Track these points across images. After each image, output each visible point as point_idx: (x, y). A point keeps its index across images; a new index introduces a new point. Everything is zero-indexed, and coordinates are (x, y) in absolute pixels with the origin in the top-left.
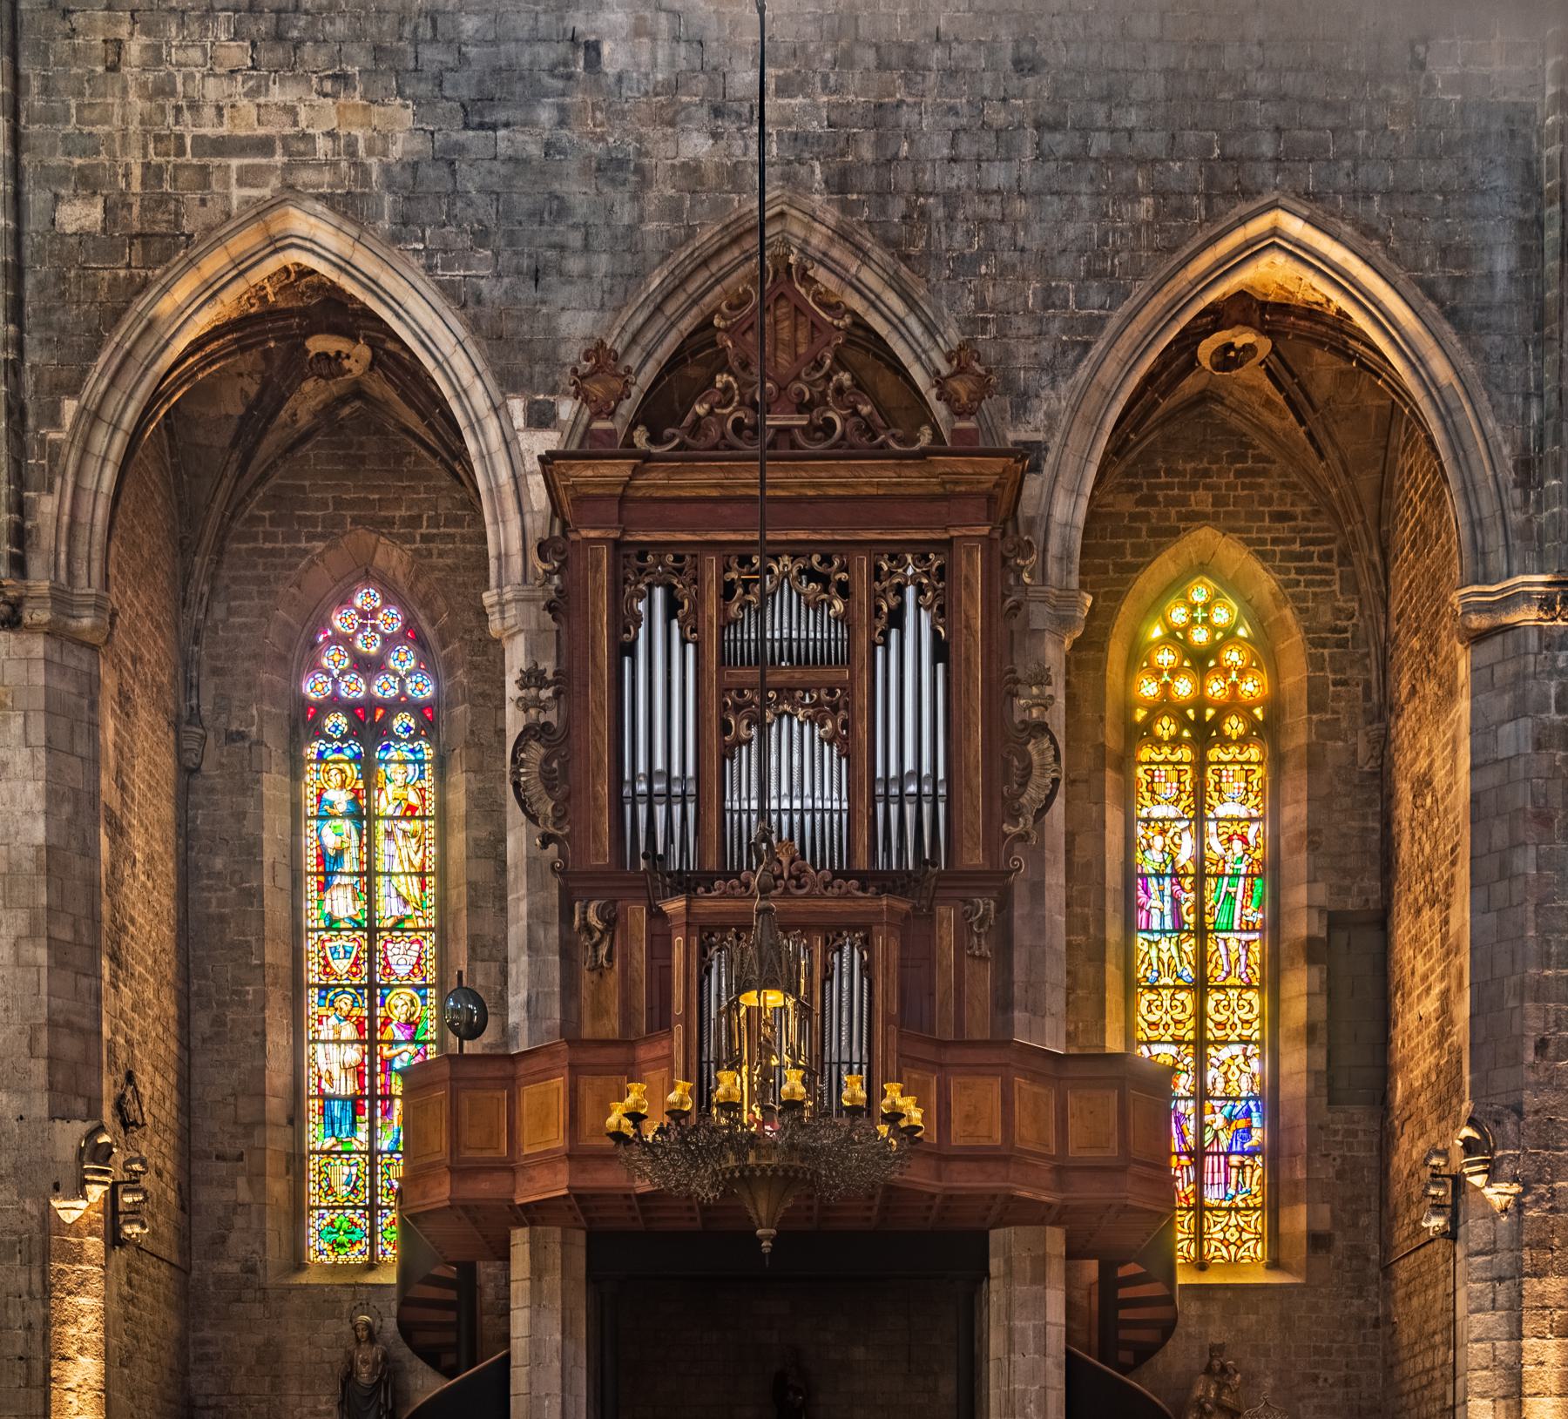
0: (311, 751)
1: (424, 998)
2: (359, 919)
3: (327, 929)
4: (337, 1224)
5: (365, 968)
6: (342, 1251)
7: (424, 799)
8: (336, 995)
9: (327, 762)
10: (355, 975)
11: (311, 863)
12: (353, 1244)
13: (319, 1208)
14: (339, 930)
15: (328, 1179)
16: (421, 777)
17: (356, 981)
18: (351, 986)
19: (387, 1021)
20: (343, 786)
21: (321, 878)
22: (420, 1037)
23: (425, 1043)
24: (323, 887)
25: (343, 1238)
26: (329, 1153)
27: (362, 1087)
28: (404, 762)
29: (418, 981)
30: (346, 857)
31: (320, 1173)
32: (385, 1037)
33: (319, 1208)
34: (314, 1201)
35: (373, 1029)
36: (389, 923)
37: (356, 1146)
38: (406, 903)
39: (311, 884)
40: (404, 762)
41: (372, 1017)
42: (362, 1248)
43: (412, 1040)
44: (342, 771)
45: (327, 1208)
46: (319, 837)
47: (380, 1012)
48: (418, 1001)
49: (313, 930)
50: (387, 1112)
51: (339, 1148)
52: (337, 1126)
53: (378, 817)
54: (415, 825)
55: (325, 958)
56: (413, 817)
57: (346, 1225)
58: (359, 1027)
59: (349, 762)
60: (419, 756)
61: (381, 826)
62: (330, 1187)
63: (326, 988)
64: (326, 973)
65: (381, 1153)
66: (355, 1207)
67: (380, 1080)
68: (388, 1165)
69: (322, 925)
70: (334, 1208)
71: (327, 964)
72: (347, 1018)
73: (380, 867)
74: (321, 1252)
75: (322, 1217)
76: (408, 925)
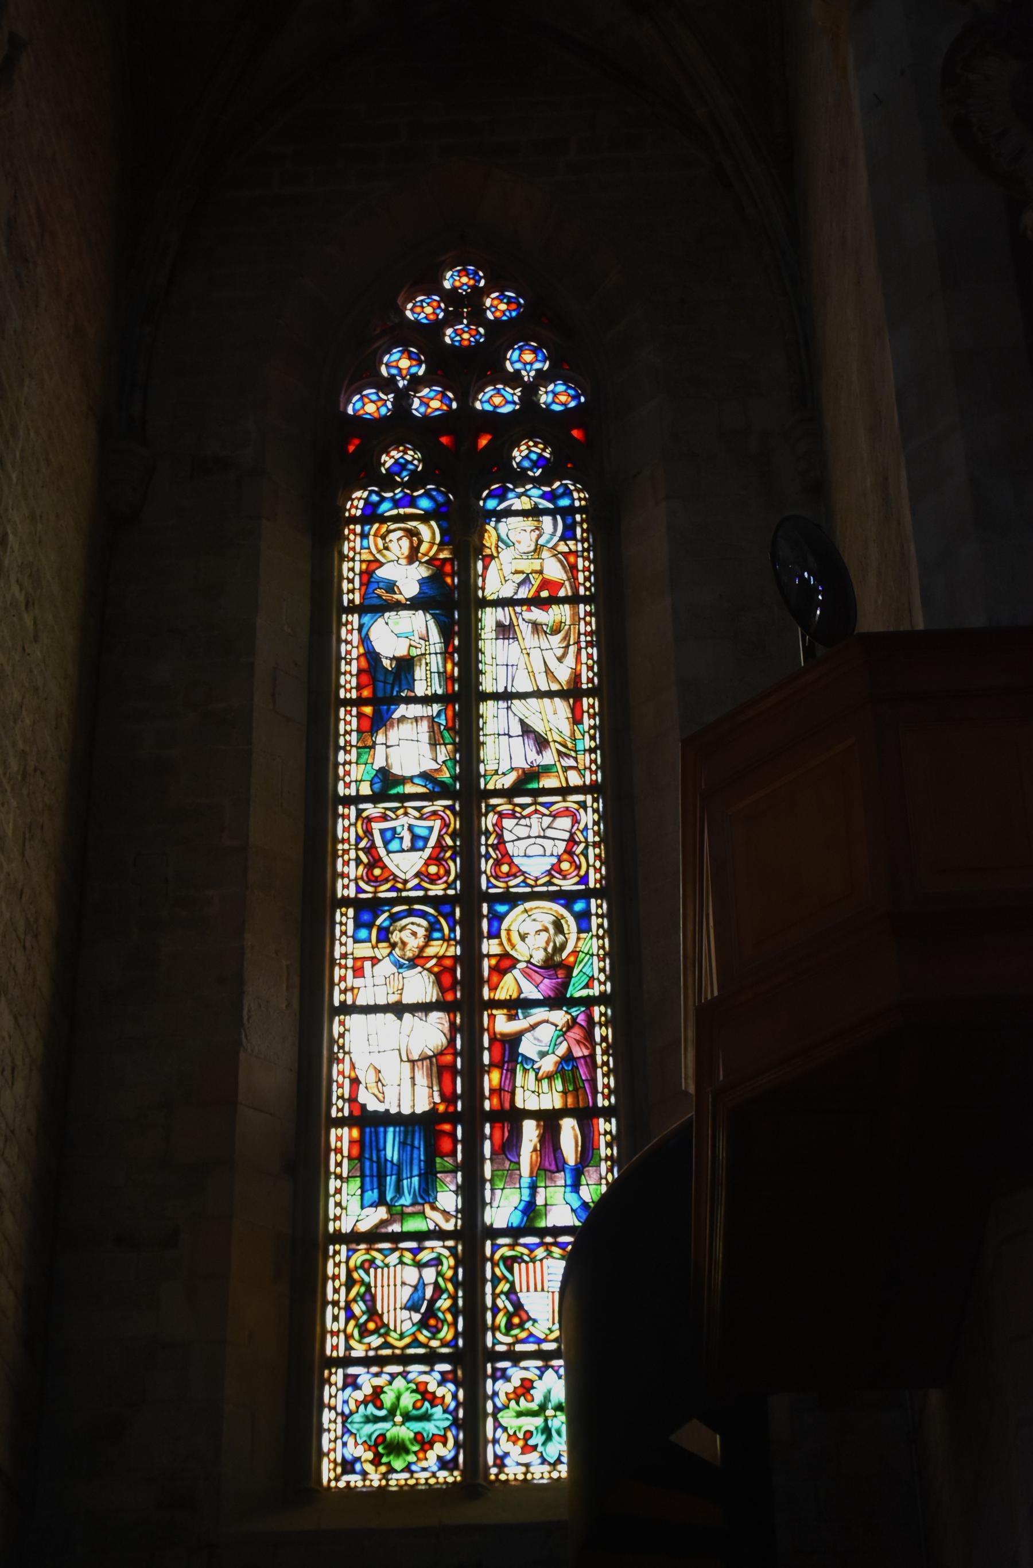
0: (357, 502)
1: (583, 919)
2: (445, 776)
3: (375, 799)
4: (388, 1399)
5: (454, 868)
6: (398, 1464)
7: (573, 569)
8: (394, 918)
9: (383, 519)
10: (433, 879)
11: (348, 685)
12: (425, 1443)
13: (347, 1361)
14: (404, 798)
15: (369, 1297)
16: (568, 534)
17: (437, 890)
18: (426, 900)
19: (506, 963)
20: (413, 556)
21: (368, 710)
22: (576, 990)
23: (588, 1002)
24: (379, 722)
25: (404, 1432)
26: (372, 1237)
27: (449, 1098)
28: (535, 513)
29: (569, 885)
30: (419, 673)
31: (350, 1283)
32: (501, 995)
33: (347, 1361)
34: (334, 1346)
35: (473, 980)
36: (508, 781)
37: (434, 1219)
38: (542, 743)
39: (348, 722)
40: (535, 513)
41: (471, 956)
42: (445, 1451)
43: (557, 1000)
44: (411, 533)
45: (365, 1362)
46: (365, 640)
47: (491, 947)
48: (570, 924)
49: (348, 801)
50: (509, 1147)
51: (396, 1228)
52: (390, 1181)
53: (485, 603)
54: (561, 613)
55: (371, 850)
56: (554, 600)
57: (408, 1401)
58: (442, 975)
59: (424, 518)
60: (564, 502)
61: (489, 618)
62: (372, 1312)
63: (375, 905)
64: (371, 880)
65: (494, 1233)
66: (431, 1358)
67: (492, 1079)
68: (509, 1262)
69: (365, 790)
70: (381, 1361)
71: (376, 861)
72: (414, 962)
73: (487, 685)
74: (348, 1466)
75: (351, 1382)
76: (549, 782)
